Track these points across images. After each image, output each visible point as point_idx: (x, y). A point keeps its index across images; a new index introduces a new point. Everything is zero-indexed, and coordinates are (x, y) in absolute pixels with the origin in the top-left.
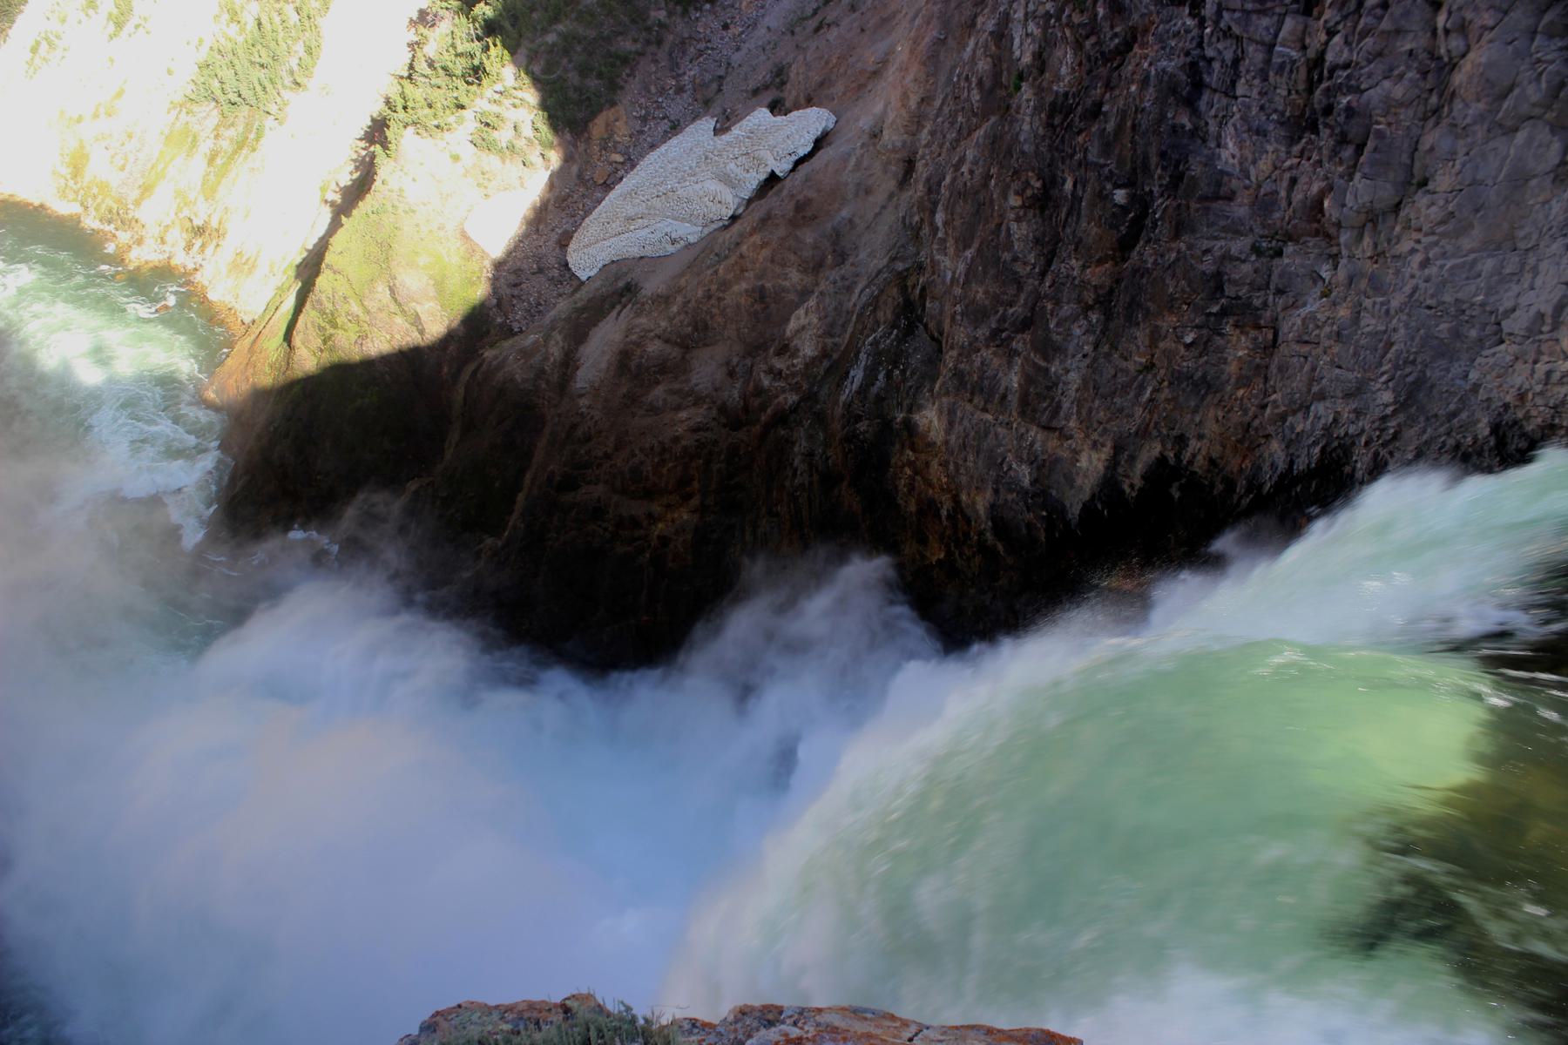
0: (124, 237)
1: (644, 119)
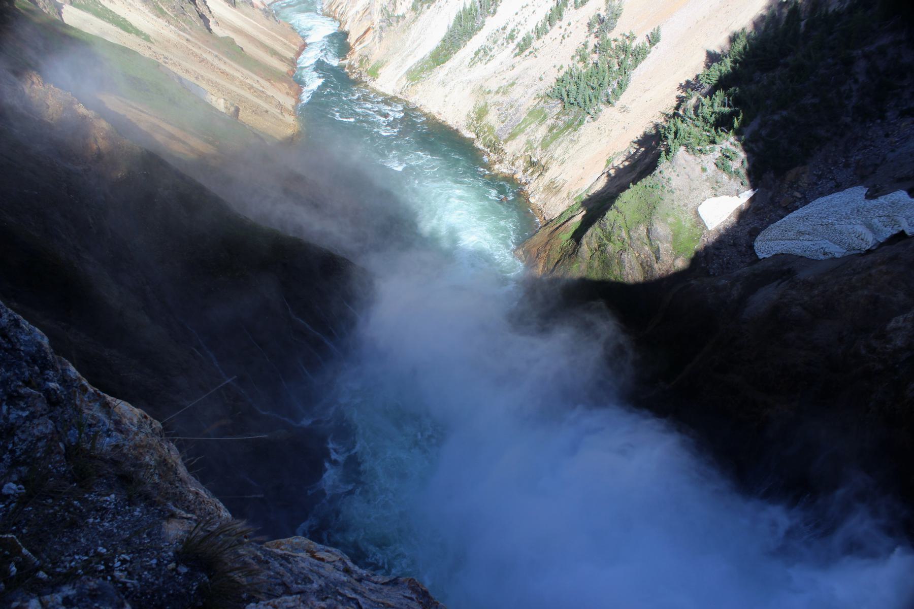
0: (493, 157)
1: (820, 177)
